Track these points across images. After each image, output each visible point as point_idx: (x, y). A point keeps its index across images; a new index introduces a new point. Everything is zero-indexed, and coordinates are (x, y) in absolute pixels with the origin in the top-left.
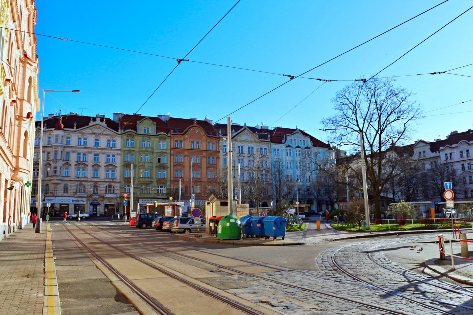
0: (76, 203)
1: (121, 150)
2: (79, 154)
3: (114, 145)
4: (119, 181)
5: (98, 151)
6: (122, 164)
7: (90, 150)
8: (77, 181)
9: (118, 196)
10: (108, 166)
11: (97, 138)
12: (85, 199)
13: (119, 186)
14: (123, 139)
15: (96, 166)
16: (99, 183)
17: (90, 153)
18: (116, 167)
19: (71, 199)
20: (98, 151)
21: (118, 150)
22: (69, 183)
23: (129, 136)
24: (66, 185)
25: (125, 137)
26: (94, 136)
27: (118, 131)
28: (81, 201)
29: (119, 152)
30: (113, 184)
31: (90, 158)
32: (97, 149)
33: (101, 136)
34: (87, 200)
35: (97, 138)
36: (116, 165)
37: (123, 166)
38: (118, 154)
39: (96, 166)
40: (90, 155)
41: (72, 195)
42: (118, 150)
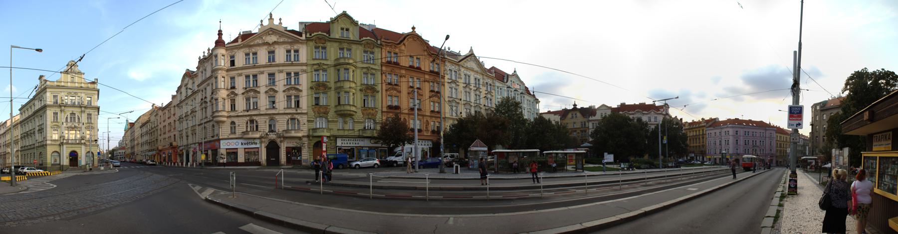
0: (246, 146)
1: (306, 65)
2: (247, 77)
3: (297, 57)
4: (306, 112)
5: (271, 70)
6: (310, 85)
7: (262, 69)
8: (246, 116)
9: (306, 134)
10: (288, 89)
11: (272, 48)
12: (258, 141)
13: (306, 119)
14: (309, 48)
15: (272, 93)
16: (277, 117)
17: (262, 73)
18: (301, 91)
19: (240, 141)
20: (271, 70)
21: (302, 65)
22: (235, 120)
23: (317, 41)
24: (233, 123)
25: (312, 44)
26: (266, 47)
27: (301, 36)
28: (252, 144)
29: (304, 68)
30: (296, 116)
31: (263, 80)
32: (271, 66)
33: (276, 46)
34: (261, 143)
35: (272, 48)
36: (300, 88)
37: (311, 88)
38: (305, 71)
39: (272, 93)
40: (261, 75)
41: (240, 136)
42: (302, 65)
